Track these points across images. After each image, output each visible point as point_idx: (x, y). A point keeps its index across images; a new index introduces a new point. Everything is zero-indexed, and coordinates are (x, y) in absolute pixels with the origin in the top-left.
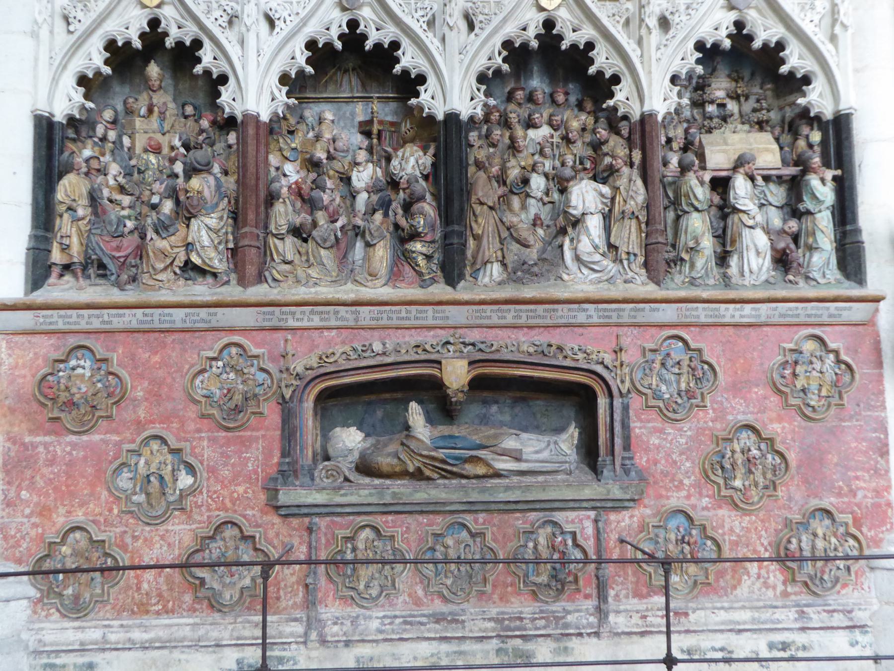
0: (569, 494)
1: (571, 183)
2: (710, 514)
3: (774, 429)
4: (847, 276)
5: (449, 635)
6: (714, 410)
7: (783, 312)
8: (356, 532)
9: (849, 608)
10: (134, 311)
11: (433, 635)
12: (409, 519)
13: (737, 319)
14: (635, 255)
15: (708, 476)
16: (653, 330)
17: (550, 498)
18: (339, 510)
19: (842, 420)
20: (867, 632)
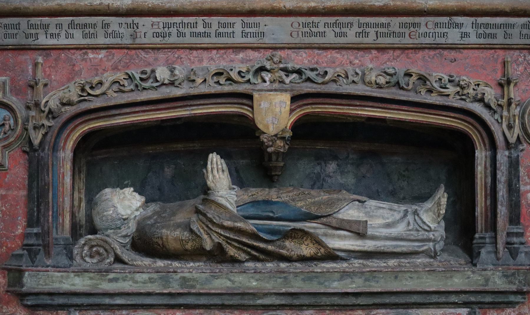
0: (431, 284)
17: (405, 289)
18: (107, 301)
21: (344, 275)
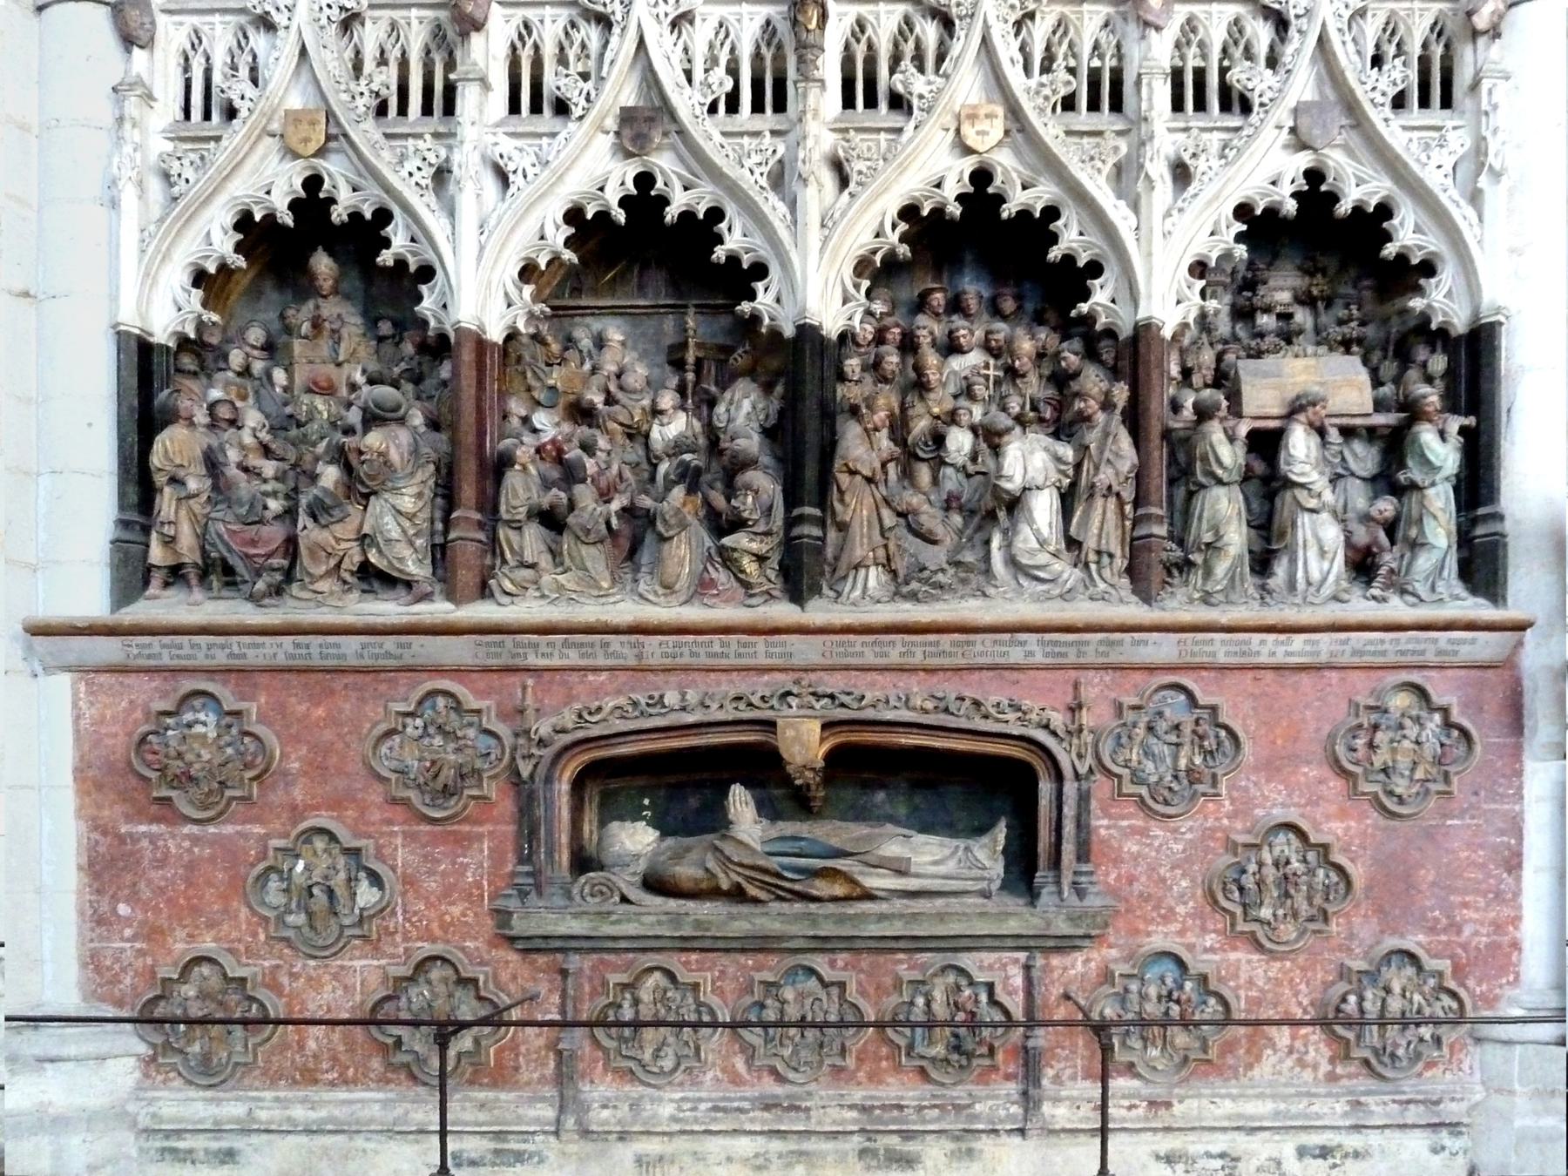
1: (1006, 438)
2: (1217, 958)
3: (1331, 829)
4: (1474, 591)
5: (783, 1128)
6: (1233, 801)
7: (1359, 646)
8: (638, 978)
9: (1435, 1098)
10: (280, 639)
11: (758, 1128)
12: (724, 960)
13: (1280, 659)
14: (1111, 556)
15: (1216, 902)
16: (1138, 677)
18: (610, 944)
19: (1445, 816)
20: (1460, 1133)
21: (882, 917)
